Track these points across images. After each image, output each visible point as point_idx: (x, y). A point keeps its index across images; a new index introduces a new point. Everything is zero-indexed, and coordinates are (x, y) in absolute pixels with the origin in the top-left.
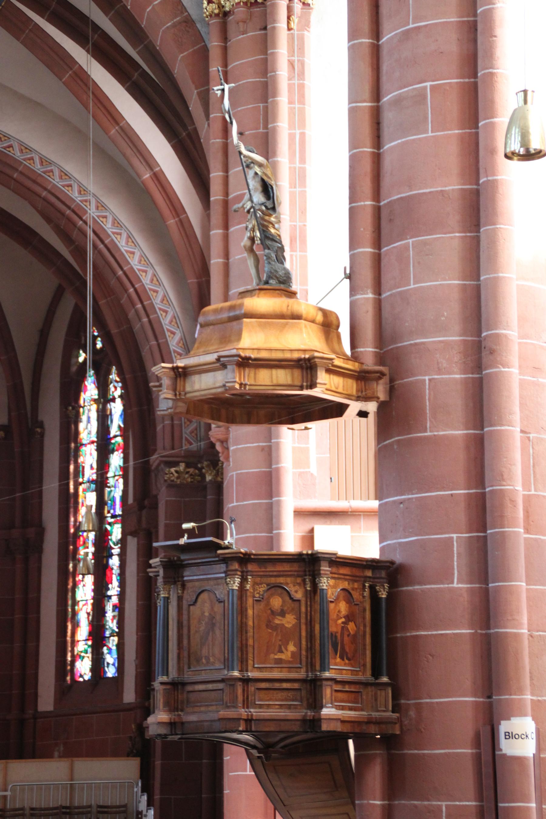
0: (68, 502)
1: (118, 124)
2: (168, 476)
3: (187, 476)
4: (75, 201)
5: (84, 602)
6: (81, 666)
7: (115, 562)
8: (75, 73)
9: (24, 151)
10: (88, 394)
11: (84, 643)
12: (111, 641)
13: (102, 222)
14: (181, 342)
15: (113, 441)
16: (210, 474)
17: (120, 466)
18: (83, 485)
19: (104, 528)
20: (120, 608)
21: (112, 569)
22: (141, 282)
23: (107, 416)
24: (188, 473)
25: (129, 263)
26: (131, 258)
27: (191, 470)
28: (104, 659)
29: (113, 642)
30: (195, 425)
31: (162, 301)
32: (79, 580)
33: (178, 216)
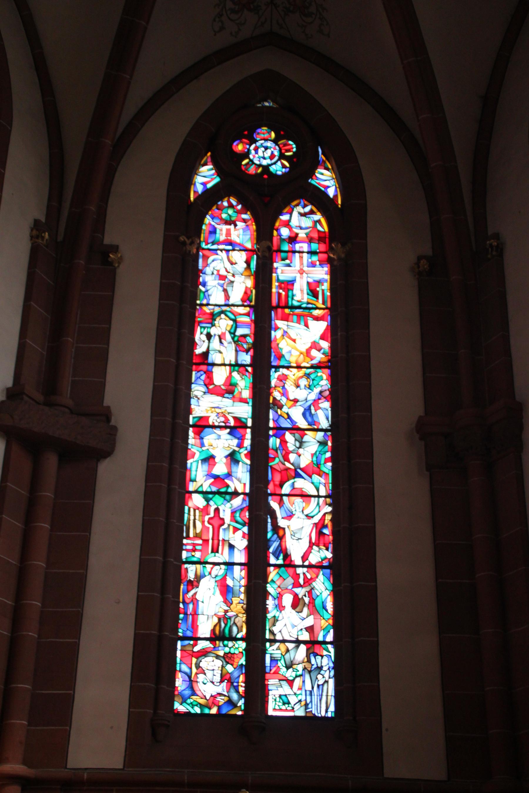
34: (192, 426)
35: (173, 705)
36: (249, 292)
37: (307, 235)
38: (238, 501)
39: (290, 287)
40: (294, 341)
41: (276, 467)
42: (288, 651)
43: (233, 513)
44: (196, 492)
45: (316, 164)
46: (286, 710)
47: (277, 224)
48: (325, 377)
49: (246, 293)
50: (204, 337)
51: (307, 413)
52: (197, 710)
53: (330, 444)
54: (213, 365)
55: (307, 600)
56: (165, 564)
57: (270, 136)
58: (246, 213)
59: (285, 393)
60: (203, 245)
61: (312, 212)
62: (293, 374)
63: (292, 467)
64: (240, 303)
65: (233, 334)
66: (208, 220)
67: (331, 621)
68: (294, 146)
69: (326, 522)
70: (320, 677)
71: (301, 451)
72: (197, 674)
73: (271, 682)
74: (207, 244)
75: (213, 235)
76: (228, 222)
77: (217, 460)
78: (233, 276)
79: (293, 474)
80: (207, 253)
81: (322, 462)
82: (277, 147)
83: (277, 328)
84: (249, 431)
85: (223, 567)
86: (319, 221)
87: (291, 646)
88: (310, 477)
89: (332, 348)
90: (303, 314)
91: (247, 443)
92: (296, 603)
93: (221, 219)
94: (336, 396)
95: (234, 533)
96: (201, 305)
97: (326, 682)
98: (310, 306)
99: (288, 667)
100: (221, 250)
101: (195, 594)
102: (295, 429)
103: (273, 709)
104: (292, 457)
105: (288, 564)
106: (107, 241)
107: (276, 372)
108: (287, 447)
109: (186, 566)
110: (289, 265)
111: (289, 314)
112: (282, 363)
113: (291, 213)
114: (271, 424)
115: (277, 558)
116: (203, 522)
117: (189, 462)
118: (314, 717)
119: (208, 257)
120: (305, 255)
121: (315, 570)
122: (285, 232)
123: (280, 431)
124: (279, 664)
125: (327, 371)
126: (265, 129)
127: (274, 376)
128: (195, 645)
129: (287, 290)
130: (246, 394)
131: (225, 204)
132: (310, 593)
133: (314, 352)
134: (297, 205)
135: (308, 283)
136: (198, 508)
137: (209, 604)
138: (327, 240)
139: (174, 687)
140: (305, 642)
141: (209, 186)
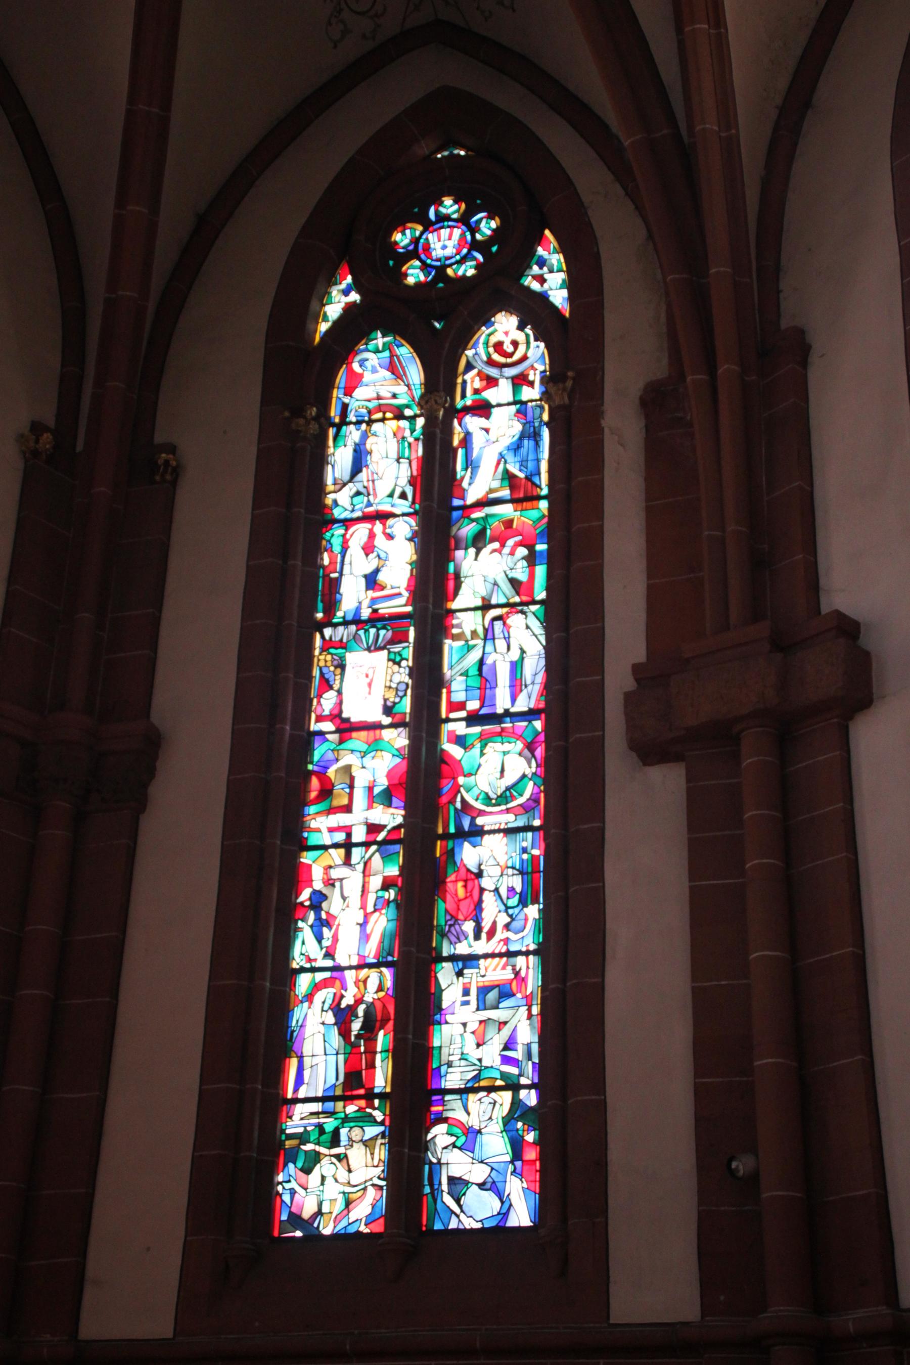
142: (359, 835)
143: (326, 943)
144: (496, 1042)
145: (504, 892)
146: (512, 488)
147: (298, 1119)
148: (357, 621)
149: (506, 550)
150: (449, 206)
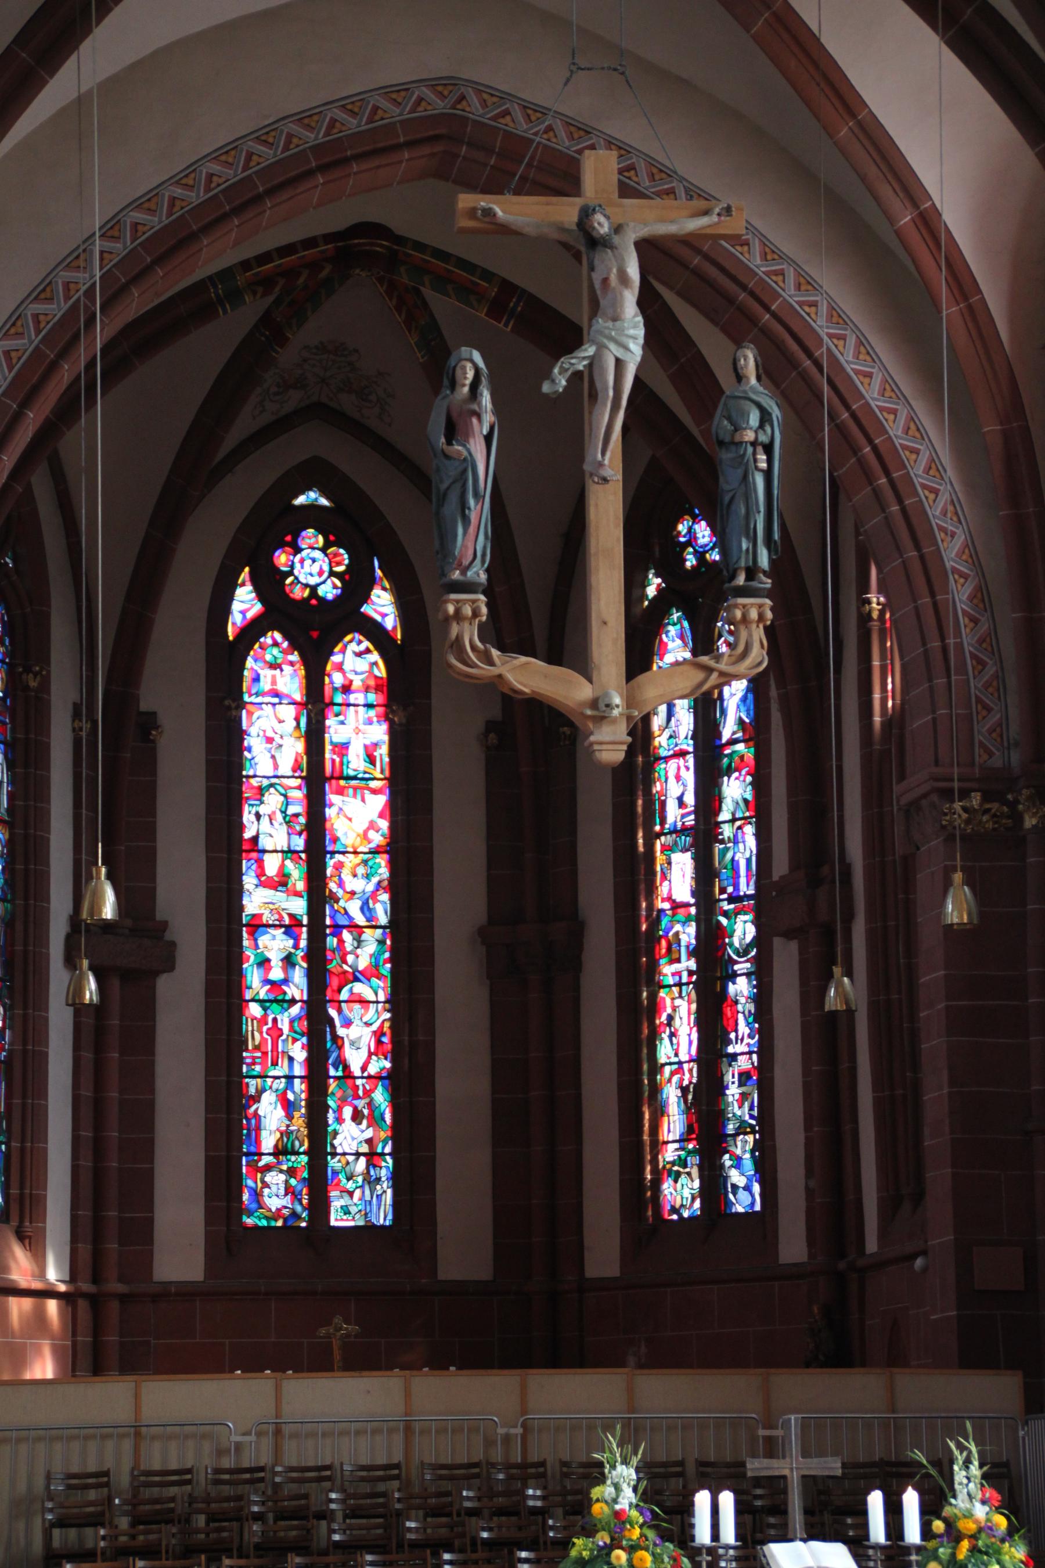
0: (637, 874)
1: (853, 115)
2: (948, 818)
3: (985, 818)
4: (757, 274)
5: (675, 1067)
6: (672, 1190)
7: (741, 988)
8: (775, 14)
9: (657, 177)
10: (669, 658)
11: (676, 1145)
12: (739, 1144)
13: (808, 314)
14: (967, 551)
15: (727, 752)
16: (1034, 815)
17: (745, 801)
18: (663, 838)
19: (714, 921)
20: (763, 1077)
21: (736, 1002)
22: (887, 433)
23: (715, 701)
24: (987, 811)
25: (863, 397)
26: (866, 386)
27: (995, 806)
28: (726, 1178)
29: (744, 1146)
30: (998, 716)
31: (927, 470)
32: (661, 1023)
33: (966, 299)
34: (245, 926)
35: (241, 1219)
36: (299, 759)
37: (364, 681)
38: (296, 1010)
39: (344, 752)
40: (350, 820)
41: (334, 970)
42: (348, 1163)
43: (292, 1022)
44: (253, 1000)
45: (371, 582)
46: (347, 1220)
47: (329, 667)
48: (383, 864)
49: (296, 760)
50: (253, 818)
51: (365, 908)
52: (264, 1223)
53: (388, 942)
54: (264, 851)
55: (366, 1112)
56: (229, 1083)
57: (317, 542)
58: (292, 654)
59: (341, 884)
60: (246, 698)
61: (367, 651)
62: (350, 861)
63: (350, 970)
64: (290, 773)
65: (284, 812)
66: (250, 662)
67: (389, 1133)
68: (346, 556)
69: (385, 1029)
70: (378, 1187)
71: (359, 951)
72: (262, 1188)
73: (332, 1194)
74: (250, 695)
75: (256, 684)
76: (274, 666)
77: (272, 963)
78: (282, 737)
79: (351, 978)
80: (249, 707)
81: (381, 963)
82: (326, 559)
83: (331, 805)
84: (304, 929)
85: (283, 1080)
86: (376, 663)
87: (351, 1158)
88: (369, 980)
89: (392, 828)
90: (360, 784)
91: (303, 943)
92: (357, 1117)
93: (265, 662)
94: (395, 886)
95: (293, 1043)
96: (248, 777)
97: (385, 1192)
98: (367, 776)
99: (348, 1179)
100: (267, 704)
101: (257, 1109)
102: (353, 927)
103: (336, 1219)
104: (350, 958)
105: (348, 1075)
106: (144, 707)
107: (331, 858)
108: (344, 948)
109: (247, 1080)
110: (342, 723)
111: (345, 787)
112: (338, 847)
113: (343, 651)
114: (328, 922)
115: (337, 1069)
116: (261, 1033)
117: (244, 966)
118: (374, 1226)
119: (252, 713)
120: (361, 709)
121: (373, 1080)
122: (338, 679)
123: (337, 929)
124: (340, 1176)
125: (385, 856)
126: (311, 531)
127: (330, 863)
128: (260, 1160)
129: (341, 755)
130: (300, 886)
131: (269, 641)
132: (370, 1105)
133: (372, 834)
134: (351, 641)
135: (366, 747)
136: (256, 1018)
137: (271, 1118)
138: (385, 689)
139: (241, 1202)
140: (364, 1154)
141: (249, 615)
142: (685, 979)
143: (675, 1047)
144: (746, 1105)
145: (747, 1013)
146: (744, 730)
147: (670, 1153)
148: (674, 831)
149: (742, 778)
150: (682, 528)
